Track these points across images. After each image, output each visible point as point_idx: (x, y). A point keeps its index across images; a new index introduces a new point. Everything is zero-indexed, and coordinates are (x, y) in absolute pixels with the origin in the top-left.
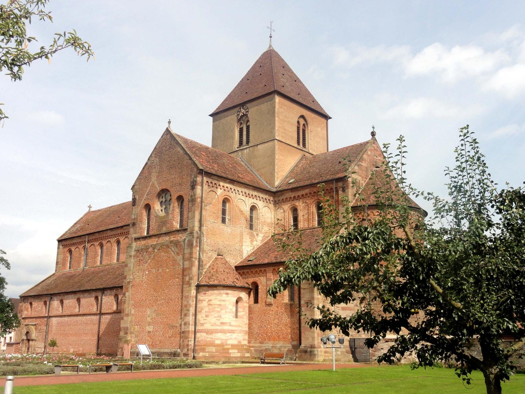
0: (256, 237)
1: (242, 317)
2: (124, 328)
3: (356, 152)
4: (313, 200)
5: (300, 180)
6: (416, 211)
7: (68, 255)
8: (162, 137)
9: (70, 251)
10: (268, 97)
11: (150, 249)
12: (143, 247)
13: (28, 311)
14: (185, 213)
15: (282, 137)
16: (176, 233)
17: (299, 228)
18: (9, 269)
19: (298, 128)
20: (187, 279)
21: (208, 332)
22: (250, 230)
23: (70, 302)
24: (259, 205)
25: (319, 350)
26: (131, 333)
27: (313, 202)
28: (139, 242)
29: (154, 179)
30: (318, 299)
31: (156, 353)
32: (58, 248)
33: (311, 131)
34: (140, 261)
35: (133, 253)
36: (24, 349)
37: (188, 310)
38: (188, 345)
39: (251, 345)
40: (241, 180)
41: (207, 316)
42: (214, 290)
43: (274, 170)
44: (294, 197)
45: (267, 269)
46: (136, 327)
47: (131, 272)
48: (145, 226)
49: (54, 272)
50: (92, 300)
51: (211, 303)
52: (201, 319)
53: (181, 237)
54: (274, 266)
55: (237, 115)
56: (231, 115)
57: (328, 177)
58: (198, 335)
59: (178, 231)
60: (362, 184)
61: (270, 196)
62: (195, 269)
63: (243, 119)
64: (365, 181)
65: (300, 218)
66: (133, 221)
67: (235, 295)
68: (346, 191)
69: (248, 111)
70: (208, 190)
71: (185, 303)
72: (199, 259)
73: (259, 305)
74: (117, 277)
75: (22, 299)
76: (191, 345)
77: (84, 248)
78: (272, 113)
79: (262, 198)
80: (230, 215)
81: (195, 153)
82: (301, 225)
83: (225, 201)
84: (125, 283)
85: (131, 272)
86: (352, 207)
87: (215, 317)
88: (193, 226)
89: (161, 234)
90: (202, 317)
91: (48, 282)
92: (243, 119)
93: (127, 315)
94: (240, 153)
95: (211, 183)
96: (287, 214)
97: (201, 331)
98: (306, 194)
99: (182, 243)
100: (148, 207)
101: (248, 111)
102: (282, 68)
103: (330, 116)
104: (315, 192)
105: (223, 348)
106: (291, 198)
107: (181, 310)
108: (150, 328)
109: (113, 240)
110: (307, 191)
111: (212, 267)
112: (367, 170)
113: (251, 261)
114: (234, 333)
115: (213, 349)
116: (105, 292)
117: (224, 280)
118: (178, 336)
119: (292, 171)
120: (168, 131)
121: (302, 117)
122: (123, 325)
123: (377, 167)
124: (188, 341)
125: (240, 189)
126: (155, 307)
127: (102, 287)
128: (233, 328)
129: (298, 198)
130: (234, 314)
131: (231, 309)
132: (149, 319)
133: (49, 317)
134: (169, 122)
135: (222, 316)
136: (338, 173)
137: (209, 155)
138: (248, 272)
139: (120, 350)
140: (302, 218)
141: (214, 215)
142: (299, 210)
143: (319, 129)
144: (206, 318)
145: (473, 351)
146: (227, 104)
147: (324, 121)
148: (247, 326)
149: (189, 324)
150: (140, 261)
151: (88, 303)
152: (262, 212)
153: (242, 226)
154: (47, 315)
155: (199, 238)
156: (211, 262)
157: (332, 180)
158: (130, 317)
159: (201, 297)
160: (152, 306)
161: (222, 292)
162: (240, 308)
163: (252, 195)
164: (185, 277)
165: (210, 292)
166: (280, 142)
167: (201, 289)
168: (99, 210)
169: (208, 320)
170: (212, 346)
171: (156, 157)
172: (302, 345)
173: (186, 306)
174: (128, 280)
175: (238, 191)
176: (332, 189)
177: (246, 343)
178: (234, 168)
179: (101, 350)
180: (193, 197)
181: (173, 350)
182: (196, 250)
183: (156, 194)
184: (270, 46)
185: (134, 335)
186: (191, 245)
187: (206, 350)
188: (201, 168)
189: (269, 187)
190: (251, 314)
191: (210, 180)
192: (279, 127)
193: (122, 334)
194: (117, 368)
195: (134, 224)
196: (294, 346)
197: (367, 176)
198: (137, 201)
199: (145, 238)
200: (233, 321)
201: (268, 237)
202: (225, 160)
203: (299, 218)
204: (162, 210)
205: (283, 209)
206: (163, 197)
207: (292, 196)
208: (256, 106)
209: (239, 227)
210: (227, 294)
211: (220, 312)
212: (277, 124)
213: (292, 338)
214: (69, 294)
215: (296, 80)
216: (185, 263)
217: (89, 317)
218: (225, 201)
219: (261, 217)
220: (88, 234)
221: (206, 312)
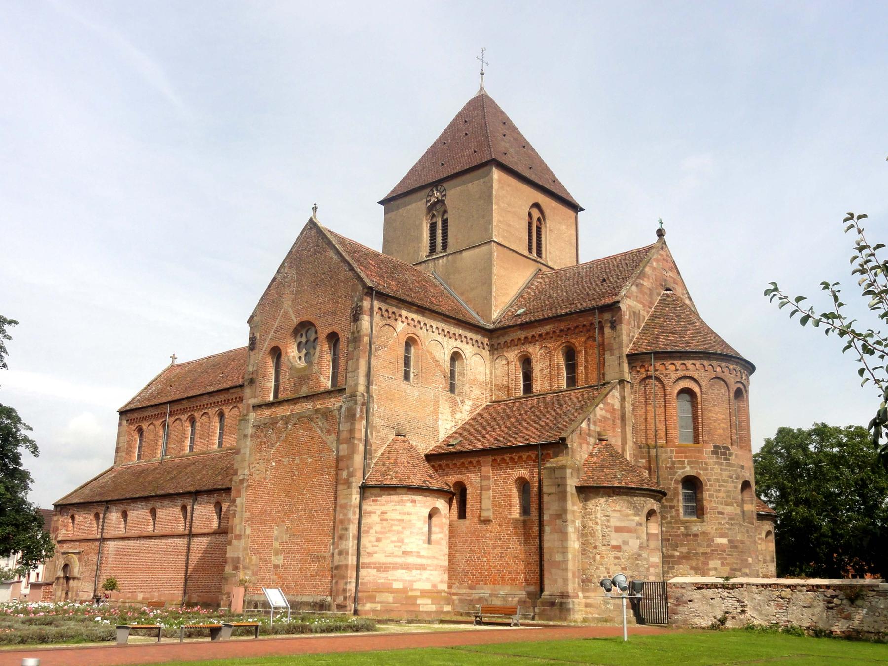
0: (461, 406)
1: (438, 543)
2: (233, 558)
3: (632, 263)
4: (559, 343)
5: (536, 310)
6: (737, 363)
7: (137, 437)
8: (302, 234)
9: (140, 431)
10: (480, 171)
12: (267, 421)
13: (67, 530)
14: (342, 362)
15: (504, 238)
17: (534, 390)
18: (37, 456)
19: (530, 224)
20: (345, 474)
21: (381, 568)
22: (450, 394)
23: (139, 514)
24: (466, 352)
25: (576, 601)
26: (245, 568)
27: (559, 347)
28: (259, 412)
30: (574, 512)
32: (120, 424)
33: (550, 230)
35: (250, 431)
36: (59, 593)
37: (347, 529)
38: (345, 590)
39: (454, 591)
40: (435, 308)
41: (378, 540)
42: (390, 495)
43: (491, 292)
44: (526, 338)
45: (482, 460)
46: (254, 557)
47: (246, 464)
48: (272, 385)
49: (112, 464)
50: (177, 511)
52: (368, 545)
53: (334, 403)
54: (512, 453)
55: (427, 202)
57: (586, 304)
58: (363, 572)
59: (328, 393)
60: (644, 317)
61: (484, 336)
62: (358, 459)
63: (437, 208)
64: (648, 312)
65: (537, 374)
66: (250, 377)
67: (427, 504)
68: (618, 327)
69: (445, 195)
70: (381, 324)
72: (366, 440)
73: (467, 522)
74: (219, 473)
75: (59, 509)
76: (350, 590)
77: (164, 424)
78: (487, 197)
79: (471, 339)
80: (417, 367)
81: (358, 261)
82: (537, 386)
83: (410, 342)
84: (236, 482)
85: (246, 464)
86: (627, 356)
87: (392, 542)
88: (356, 385)
89: (299, 398)
90: (370, 542)
91: (103, 480)
92: (437, 208)
93: (239, 537)
94: (431, 265)
95: (387, 311)
96: (512, 367)
98: (547, 333)
99: (336, 413)
100: (276, 353)
101: (445, 195)
102: (501, 125)
103: (581, 205)
104: (562, 330)
105: (406, 597)
106: (519, 339)
107: (334, 529)
108: (278, 560)
109: (213, 411)
110: (548, 328)
111: (387, 455)
112: (651, 294)
114: (425, 569)
115: (390, 598)
116: (199, 499)
117: (409, 478)
118: (328, 574)
119: (520, 296)
120: (312, 224)
121: (536, 205)
122: (230, 553)
123: (668, 289)
124: (346, 583)
125: (435, 324)
126: (288, 524)
127: (193, 489)
128: (424, 561)
129: (532, 340)
130: (425, 538)
131: (421, 529)
132: (276, 544)
133: (103, 540)
134: (315, 209)
135: (406, 541)
136: (603, 298)
137: (382, 266)
138: (448, 465)
139: (225, 597)
140: (539, 374)
141: (391, 366)
142: (534, 361)
143: (564, 227)
144: (377, 543)
145: (860, 607)
147: (571, 213)
148: (447, 558)
149: (347, 553)
151: (170, 516)
152: (470, 364)
153: (437, 387)
154: (99, 536)
155: (366, 404)
156: (385, 446)
157: (593, 309)
158: (243, 541)
159: (368, 506)
160: (283, 522)
161: (405, 498)
162: (435, 526)
163: (454, 334)
164: (340, 472)
165: (384, 498)
166: (500, 247)
167: (368, 493)
168: (189, 363)
169: (380, 548)
171: (291, 267)
172: (546, 593)
173: (342, 522)
174: (241, 477)
175: (431, 326)
176: (592, 324)
177: (444, 587)
178: (423, 287)
179: (190, 598)
180: (356, 335)
181: (318, 599)
183: (291, 330)
184: (482, 89)
185: (249, 572)
186: (351, 417)
187: (377, 600)
188: (370, 284)
189: (482, 322)
190: (454, 537)
191: (384, 307)
192: (499, 221)
193: (228, 569)
194: (230, 630)
195: (252, 382)
196: (529, 594)
197: (652, 303)
198: (258, 342)
199: (270, 405)
200: (424, 548)
201: (480, 406)
202: (408, 275)
203: (534, 375)
204: (300, 358)
205: (506, 359)
206: (302, 335)
207: (523, 337)
208: (459, 186)
209: (432, 389)
210: (414, 501)
211: (402, 533)
212: (496, 217)
213: (526, 580)
214: (136, 502)
215: (525, 145)
216: (341, 447)
217: (170, 540)
218: (410, 342)
219: (468, 373)
220: (169, 402)
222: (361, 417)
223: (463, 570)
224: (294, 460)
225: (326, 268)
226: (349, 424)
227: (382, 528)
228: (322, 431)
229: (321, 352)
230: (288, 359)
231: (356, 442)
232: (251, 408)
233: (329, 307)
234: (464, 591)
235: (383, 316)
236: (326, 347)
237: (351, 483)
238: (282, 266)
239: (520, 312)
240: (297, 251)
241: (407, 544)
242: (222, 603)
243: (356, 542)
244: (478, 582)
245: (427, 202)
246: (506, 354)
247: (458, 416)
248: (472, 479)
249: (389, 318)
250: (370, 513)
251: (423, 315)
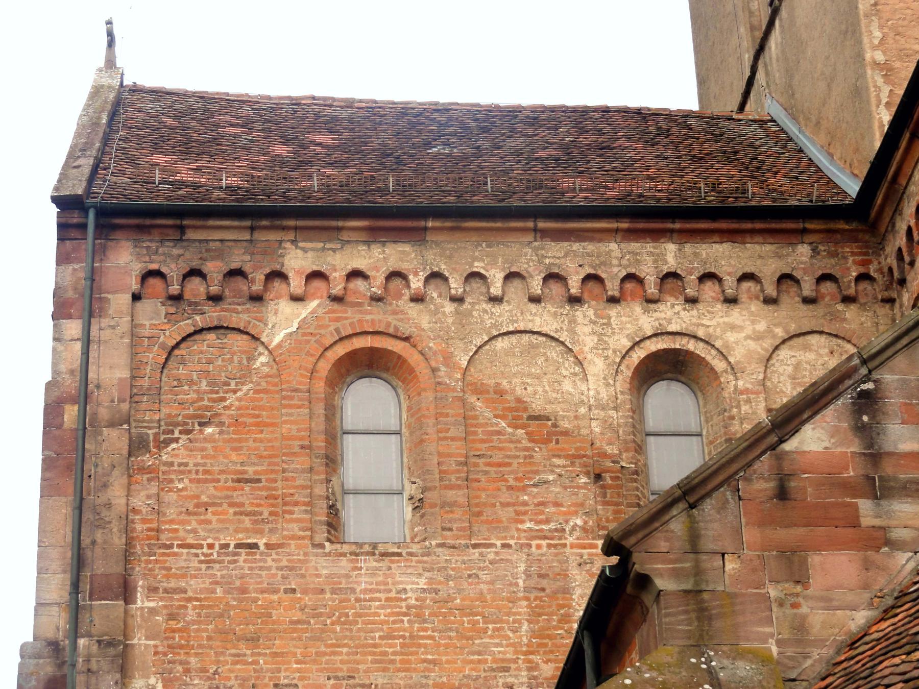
70: (171, 336)
235: (177, 298)
249: (216, 299)
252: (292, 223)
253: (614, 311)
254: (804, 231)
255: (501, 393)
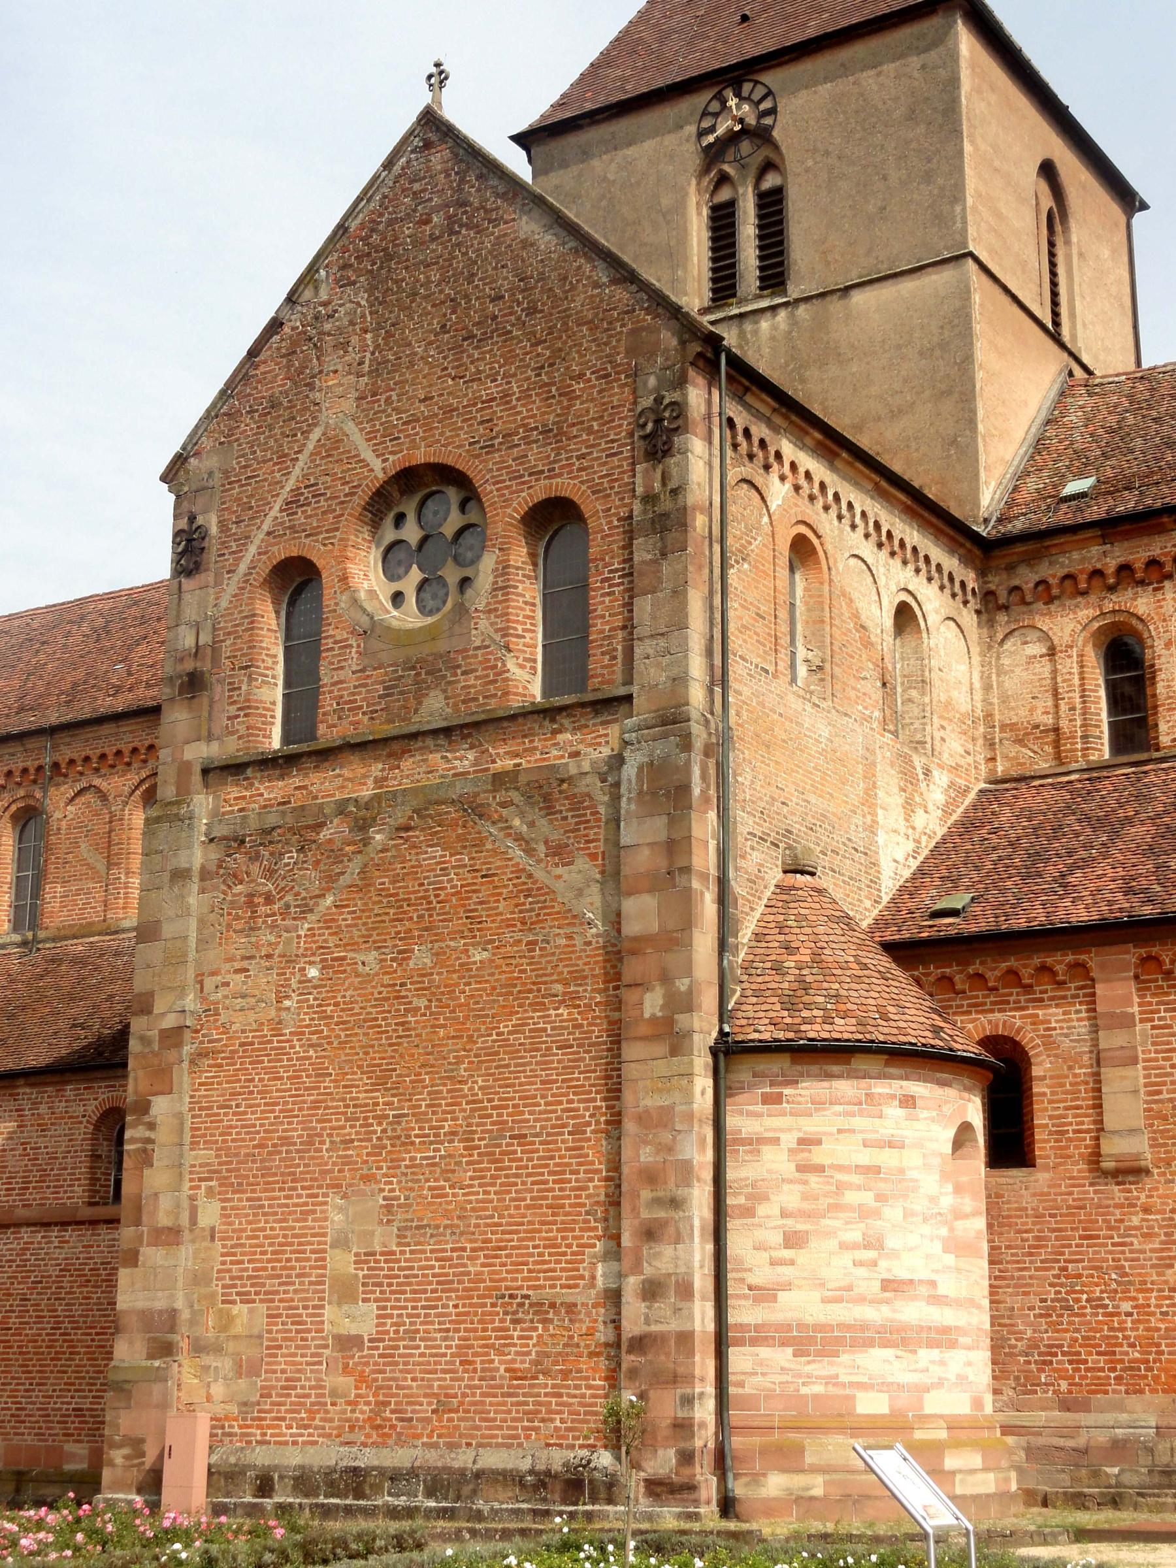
2: (147, 1318)
5: (1148, 479)
8: (388, 164)
11: (334, 831)
12: (272, 820)
15: (991, 251)
16: (531, 724)
20: (652, 1003)
21: (807, 1341)
26: (198, 1348)
29: (337, 406)
31: (413, 1472)
33: (1081, 255)
34: (250, 903)
35: (197, 856)
37: (675, 1203)
41: (793, 1240)
42: (830, 1076)
43: (972, 422)
44: (1125, 569)
45: (1093, 959)
47: (191, 974)
48: (272, 693)
51: (818, 1156)
53: (581, 749)
55: (701, 134)
56: (656, 133)
58: (739, 1359)
59: (547, 713)
61: (966, 560)
62: (704, 943)
66: (189, 666)
69: (772, 111)
71: (647, 1155)
72: (723, 882)
76: (703, 1425)
84: (143, 1039)
87: (844, 1246)
88: (680, 680)
89: (414, 736)
90: (759, 1247)
93: (170, 1236)
96: (1069, 665)
97: (760, 1336)
100: (296, 580)
101: (772, 111)
106: (1097, 573)
107: (614, 1202)
108: (360, 1319)
113: (954, 913)
114: (952, 1344)
119: (1039, 445)
120: (432, 127)
121: (1048, 170)
122: (132, 1294)
124: (688, 1401)
131: (933, 1199)
132: (342, 1262)
134: (438, 78)
135: (891, 1243)
139: (118, 1456)
141: (760, 626)
142: (1159, 645)
143: (1106, 253)
144: (787, 1254)
146: (626, 80)
149: (686, 1291)
150: (250, 903)
155: (720, 748)
156: (761, 909)
158: (185, 1256)
160: (367, 1179)
161: (881, 1088)
163: (902, 544)
165: (808, 1090)
166: (984, 278)
167: (743, 1071)
169: (796, 1269)
170: (841, 1430)
171: (344, 283)
173: (651, 1177)
174: (170, 1022)
181: (557, 1459)
182: (704, 826)
183: (361, 498)
186: (669, 794)
187: (809, 1459)
193: (128, 1352)
195: (193, 684)
199: (272, 764)
204: (397, 598)
205: (1046, 637)
206: (400, 519)
207: (1111, 564)
208: (826, 80)
210: (908, 1102)
211: (876, 1214)
216: (630, 905)
219: (935, 676)
221: (784, 1214)
222: (706, 799)
223: (1033, 1345)
224: (404, 955)
225: (506, 280)
226: (661, 822)
227: (805, 1197)
228: (530, 852)
229: (503, 569)
230: (355, 601)
231: (696, 884)
232: (197, 778)
233: (533, 411)
234: (1040, 1417)
236: (519, 554)
237: (689, 1034)
238: (308, 277)
239: (1074, 487)
240: (372, 226)
241: (895, 1254)
242: (107, 1474)
243: (710, 1247)
244: (1100, 1387)
245: (701, 134)
246: (1043, 623)
247: (920, 819)
248: (1053, 1031)
250: (756, 1143)
251: (833, 468)
252: (794, 418)
253: (891, 561)
254: (962, 545)
255: (851, 600)
